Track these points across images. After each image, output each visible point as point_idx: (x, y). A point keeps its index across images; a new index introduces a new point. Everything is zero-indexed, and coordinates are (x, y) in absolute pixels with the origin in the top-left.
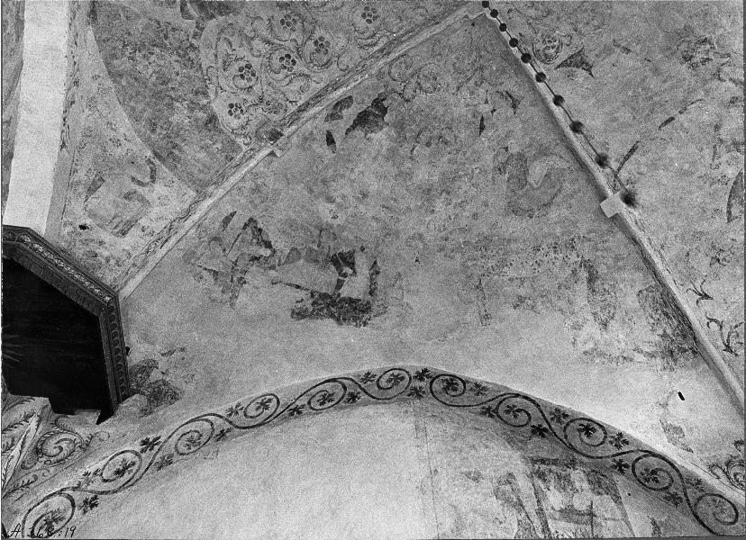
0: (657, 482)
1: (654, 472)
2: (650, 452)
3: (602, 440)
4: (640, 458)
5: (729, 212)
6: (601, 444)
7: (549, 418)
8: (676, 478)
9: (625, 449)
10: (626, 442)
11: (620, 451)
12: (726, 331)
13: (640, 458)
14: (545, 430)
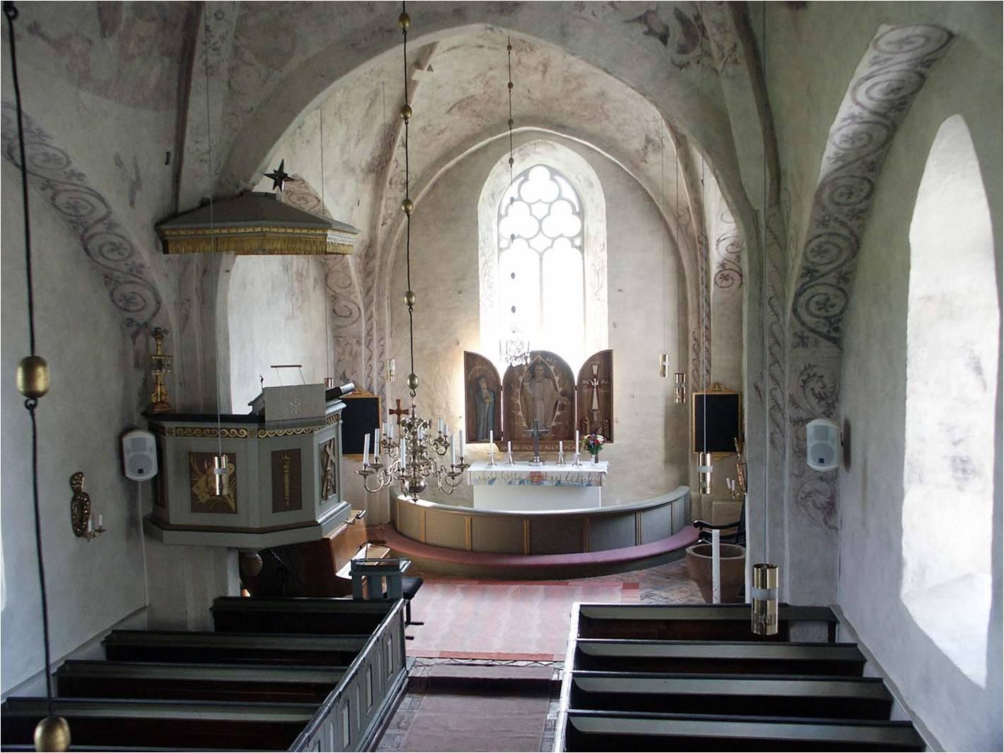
5: (451, 109)
12: (398, 170)
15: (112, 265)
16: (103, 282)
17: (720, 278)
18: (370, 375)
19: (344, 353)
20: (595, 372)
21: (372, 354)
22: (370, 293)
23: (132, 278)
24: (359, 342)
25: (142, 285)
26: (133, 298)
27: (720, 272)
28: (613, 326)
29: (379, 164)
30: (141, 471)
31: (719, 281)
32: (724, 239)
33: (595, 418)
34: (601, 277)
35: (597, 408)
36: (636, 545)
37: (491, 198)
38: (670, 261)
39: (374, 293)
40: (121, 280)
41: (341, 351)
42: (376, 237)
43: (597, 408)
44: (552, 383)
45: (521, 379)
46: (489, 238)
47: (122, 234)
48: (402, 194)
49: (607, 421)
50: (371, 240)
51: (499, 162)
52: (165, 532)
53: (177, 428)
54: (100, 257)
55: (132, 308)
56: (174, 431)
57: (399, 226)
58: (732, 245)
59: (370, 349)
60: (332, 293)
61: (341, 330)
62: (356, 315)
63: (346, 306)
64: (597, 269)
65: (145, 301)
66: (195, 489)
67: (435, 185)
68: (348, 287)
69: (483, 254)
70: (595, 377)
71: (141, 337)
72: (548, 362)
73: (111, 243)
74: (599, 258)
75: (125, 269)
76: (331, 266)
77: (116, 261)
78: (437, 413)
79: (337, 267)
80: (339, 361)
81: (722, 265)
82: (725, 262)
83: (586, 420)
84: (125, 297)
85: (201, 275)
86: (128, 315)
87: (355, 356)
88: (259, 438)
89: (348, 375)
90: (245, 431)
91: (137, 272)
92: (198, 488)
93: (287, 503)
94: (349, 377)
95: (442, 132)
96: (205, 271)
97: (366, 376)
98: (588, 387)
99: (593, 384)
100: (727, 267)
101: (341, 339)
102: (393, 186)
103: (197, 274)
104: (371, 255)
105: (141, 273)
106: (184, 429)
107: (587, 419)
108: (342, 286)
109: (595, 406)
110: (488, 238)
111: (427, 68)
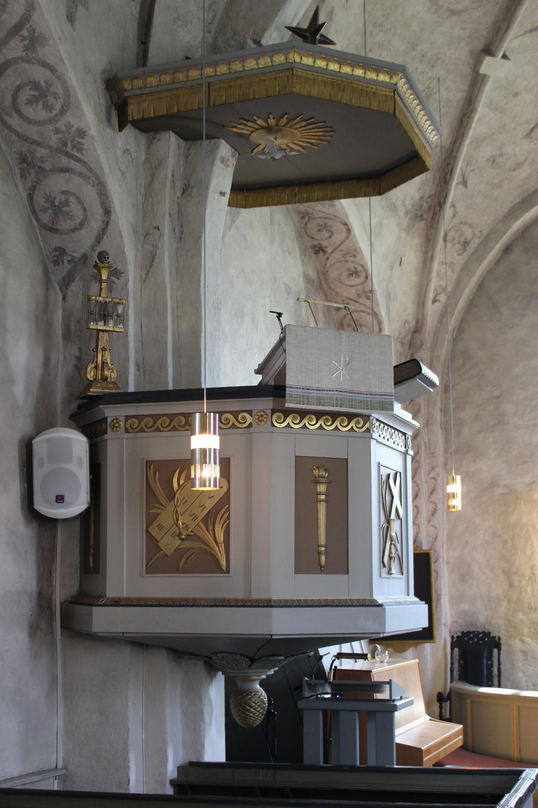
3: (353, 284)
4: (363, 312)
6: (350, 286)
7: (343, 247)
11: (357, 299)
12: (456, 221)
13: (363, 312)
14: (324, 252)
15: (33, 132)
16: (17, 172)
21: (419, 490)
23: (64, 161)
25: (80, 175)
26: (67, 203)
29: (430, 208)
30: (60, 499)
40: (47, 166)
42: (423, 317)
47: (50, 60)
48: (461, 257)
50: (418, 322)
52: (95, 610)
53: (127, 418)
54: (15, 116)
55: (65, 225)
56: (122, 424)
57: (457, 303)
65: (85, 210)
66: (154, 531)
67: (507, 250)
71: (76, 286)
73: (35, 85)
75: (54, 141)
77: (39, 123)
78: (516, 583)
84: (52, 202)
85: (178, 193)
86: (57, 241)
88: (273, 425)
90: (248, 416)
91: (73, 147)
92: (160, 527)
93: (323, 558)
95: (518, 166)
96: (186, 189)
102: (449, 245)
103: (173, 188)
104: (418, 343)
105: (79, 147)
106: (140, 418)
111: (501, 54)
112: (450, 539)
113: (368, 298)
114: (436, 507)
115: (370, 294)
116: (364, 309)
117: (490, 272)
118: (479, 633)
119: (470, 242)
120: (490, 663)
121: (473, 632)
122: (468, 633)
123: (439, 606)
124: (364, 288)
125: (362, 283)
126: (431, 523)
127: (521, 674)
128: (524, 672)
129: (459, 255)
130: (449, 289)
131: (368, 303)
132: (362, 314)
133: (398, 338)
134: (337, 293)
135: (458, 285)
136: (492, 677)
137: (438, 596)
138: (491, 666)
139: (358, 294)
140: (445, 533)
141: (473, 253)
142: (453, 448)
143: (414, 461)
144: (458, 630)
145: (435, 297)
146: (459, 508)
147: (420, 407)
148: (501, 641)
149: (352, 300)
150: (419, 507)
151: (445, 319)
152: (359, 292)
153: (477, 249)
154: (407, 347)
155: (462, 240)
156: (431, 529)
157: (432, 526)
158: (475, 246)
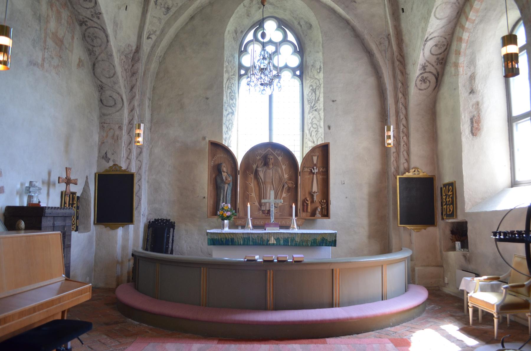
0: (93, 41)
1: (96, 37)
2: (104, 30)
3: (88, 7)
4: (96, 28)
8: (103, 47)
9: (95, 19)
10: (98, 18)
11: (92, 18)
13: (96, 28)
17: (421, 80)
18: (129, 158)
19: (107, 136)
20: (315, 162)
22: (134, 90)
24: (120, 128)
27: (421, 74)
28: (327, 128)
31: (419, 83)
32: (431, 39)
33: (315, 198)
34: (317, 93)
35: (316, 191)
36: (382, 300)
37: (235, 34)
38: (371, 81)
39: (136, 90)
41: (105, 135)
43: (316, 191)
44: (280, 171)
45: (254, 166)
46: (232, 61)
48: (165, 16)
49: (325, 201)
50: (137, 47)
51: (242, 4)
58: (436, 45)
59: (130, 135)
60: (100, 83)
61: (106, 117)
62: (119, 105)
63: (111, 97)
64: (314, 88)
67: (192, 18)
68: (112, 77)
69: (227, 71)
70: (315, 165)
72: (277, 154)
74: (316, 79)
76: (97, 54)
79: (102, 55)
80: (103, 143)
81: (424, 67)
82: (427, 64)
83: (307, 200)
87: (117, 139)
89: (109, 156)
94: (110, 157)
97: (125, 158)
98: (309, 174)
99: (313, 171)
100: (427, 70)
101: (105, 125)
102: (158, 7)
107: (308, 199)
108: (107, 76)
109: (315, 188)
110: (231, 61)
112: (150, 169)
113: (98, 18)
114: (142, 150)
115: (98, 15)
116: (96, 25)
117: (183, 28)
118: (164, 220)
119: (171, 8)
120: (168, 235)
121: (161, 219)
122: (158, 220)
123: (140, 204)
124: (95, 11)
125: (94, 7)
126: (138, 159)
127: (184, 242)
128: (186, 241)
129: (164, 14)
130: (158, 33)
131: (98, 21)
132: (95, 29)
133: (122, 52)
134: (79, 13)
135: (163, 32)
136: (169, 243)
137: (140, 199)
138: (168, 238)
139: (92, 15)
140: (148, 166)
141: (172, 15)
142: (155, 121)
143: (130, 123)
144: (153, 218)
145: (149, 36)
146: (141, 143)
147: (135, 94)
148: (175, 224)
149: (88, 18)
150: (131, 150)
151: (154, 49)
152: (92, 14)
153: (174, 13)
154: (130, 60)
155: (166, 6)
156: (138, 162)
157: (139, 160)
158: (174, 11)
